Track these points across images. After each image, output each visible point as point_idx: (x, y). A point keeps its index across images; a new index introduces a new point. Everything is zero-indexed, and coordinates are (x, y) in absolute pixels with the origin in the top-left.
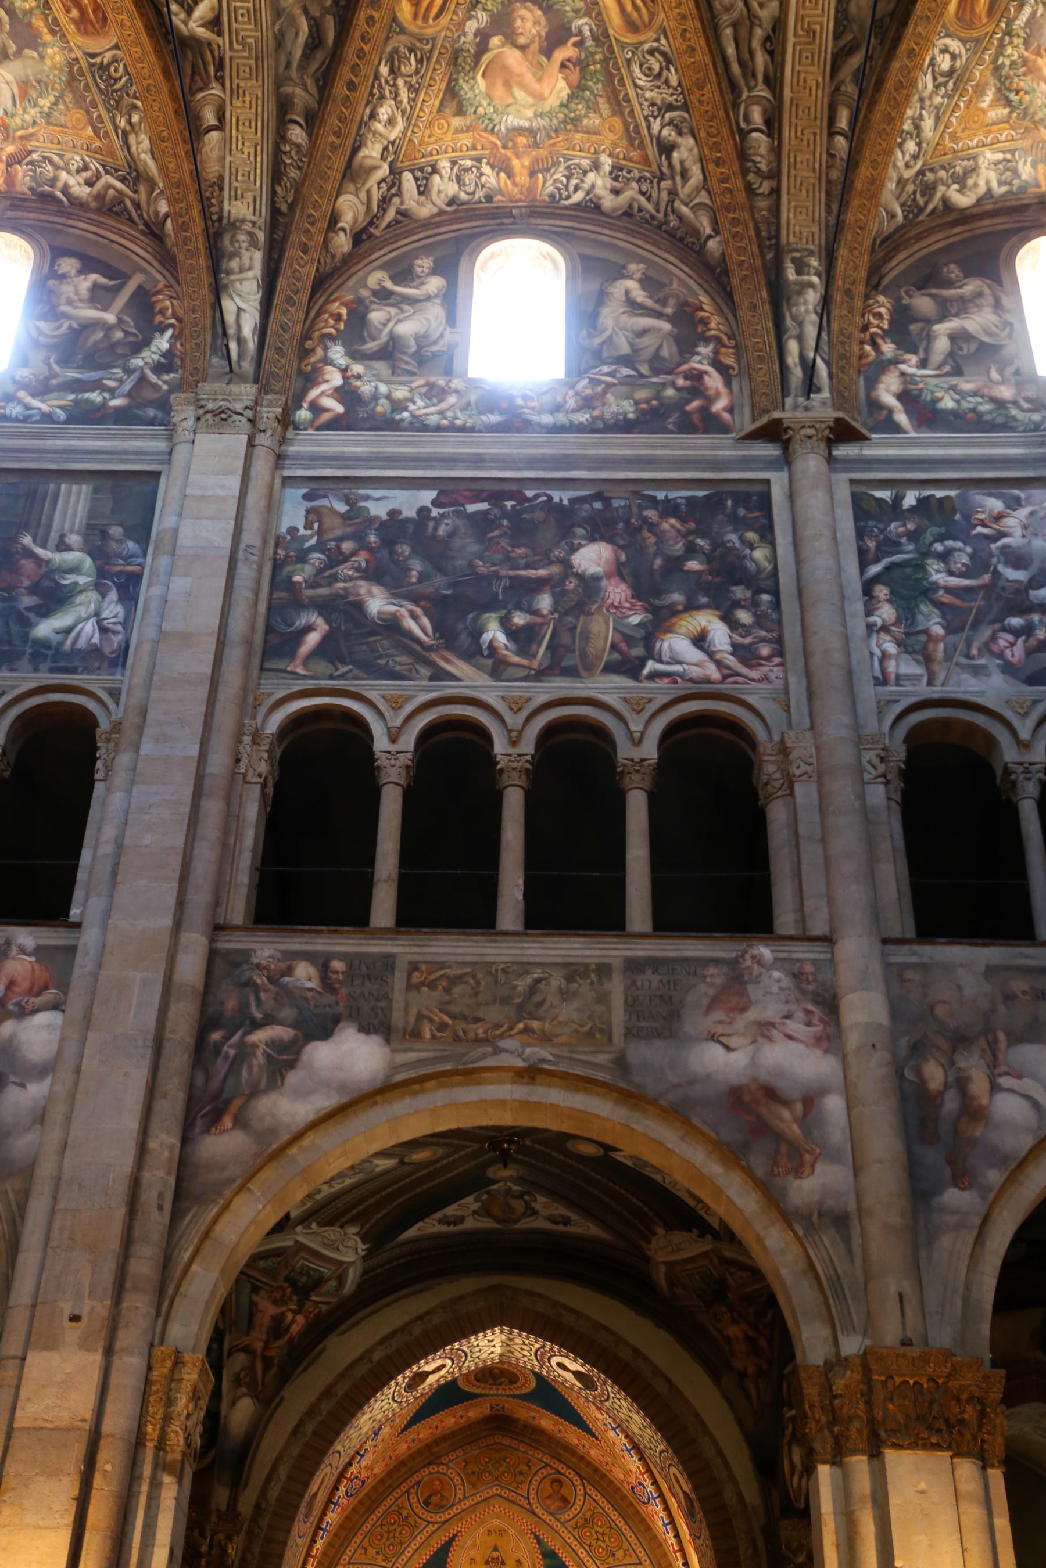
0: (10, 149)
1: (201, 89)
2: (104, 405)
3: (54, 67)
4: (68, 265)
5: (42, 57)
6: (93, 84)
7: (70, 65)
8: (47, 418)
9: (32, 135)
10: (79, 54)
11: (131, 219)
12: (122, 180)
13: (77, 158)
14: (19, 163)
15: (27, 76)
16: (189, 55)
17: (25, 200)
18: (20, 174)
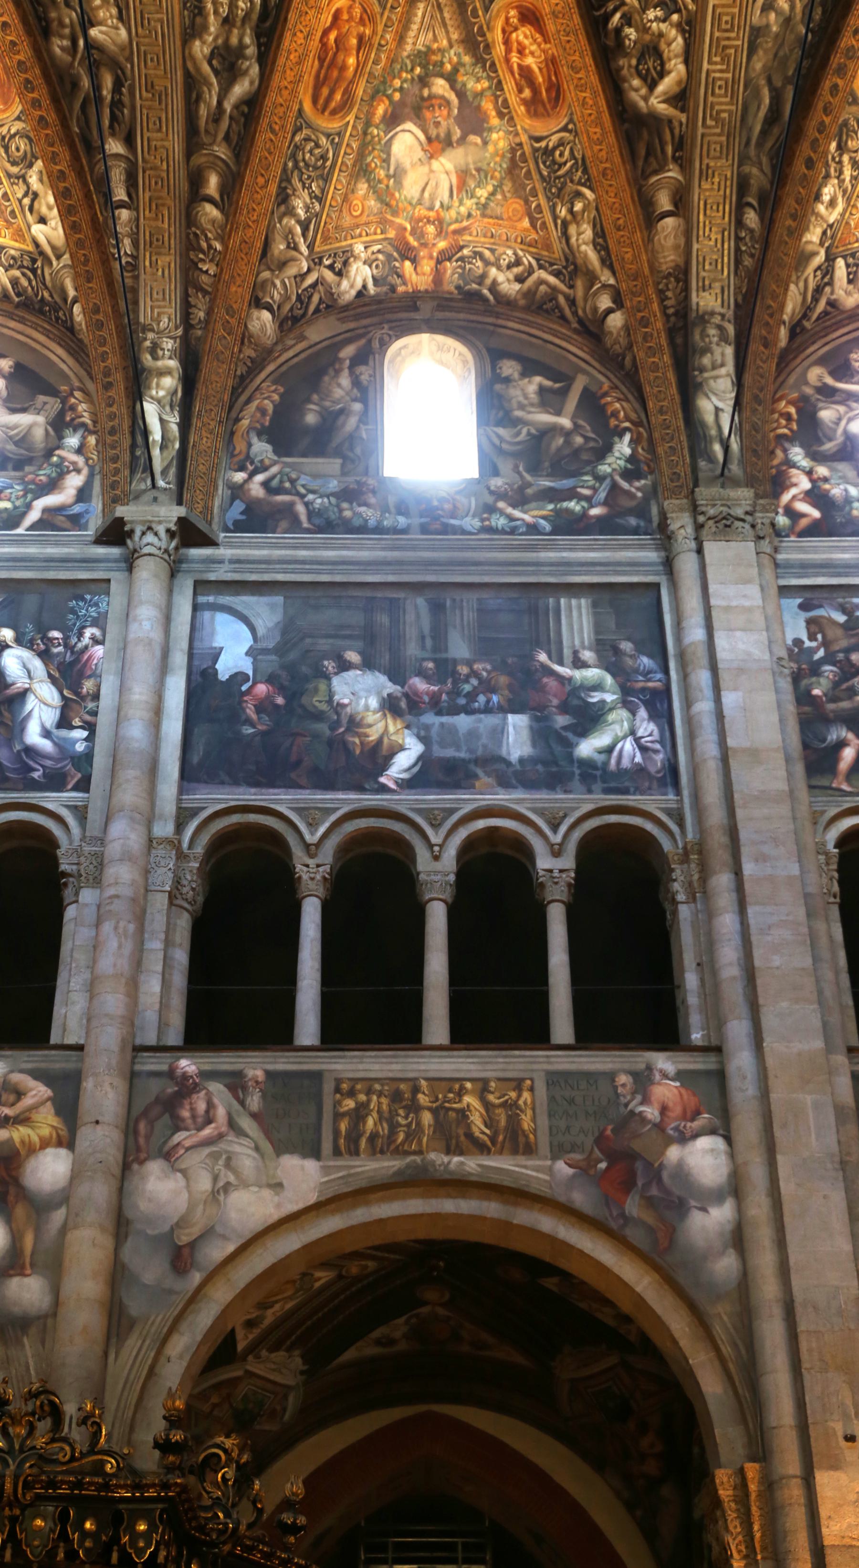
0: (442, 245)
2: (584, 514)
3: (496, 153)
4: (509, 368)
5: (485, 143)
6: (538, 172)
7: (513, 151)
8: (533, 529)
9: (465, 229)
10: (524, 138)
12: (557, 274)
13: (510, 252)
14: (449, 259)
15: (467, 164)
17: (451, 300)
18: (449, 272)
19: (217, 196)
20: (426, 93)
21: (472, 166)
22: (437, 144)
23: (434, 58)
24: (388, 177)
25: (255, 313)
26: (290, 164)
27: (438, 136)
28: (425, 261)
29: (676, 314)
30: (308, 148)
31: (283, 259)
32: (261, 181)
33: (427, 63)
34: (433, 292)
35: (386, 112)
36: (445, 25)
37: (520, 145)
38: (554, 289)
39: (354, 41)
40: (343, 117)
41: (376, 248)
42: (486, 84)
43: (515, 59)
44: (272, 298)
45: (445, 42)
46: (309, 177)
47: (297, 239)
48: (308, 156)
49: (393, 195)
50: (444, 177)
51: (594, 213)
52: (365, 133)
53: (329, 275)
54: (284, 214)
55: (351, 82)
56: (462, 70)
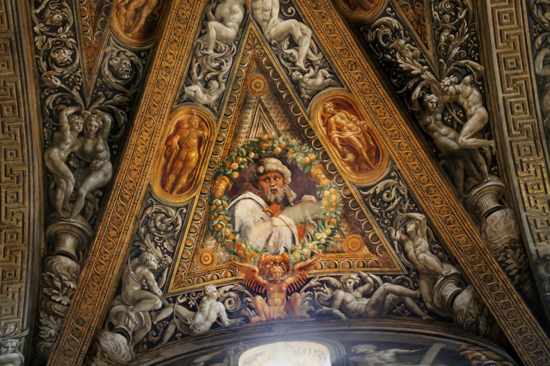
0: (290, 280)
1: (476, 186)
3: (330, 205)
5: (319, 199)
9: (310, 265)
10: (353, 190)
11: (414, 315)
12: (401, 283)
13: (354, 276)
14: (298, 291)
15: (305, 217)
16: (461, 164)
19: (73, 252)
20: (261, 169)
21: (310, 218)
22: (276, 206)
23: (265, 145)
24: (234, 233)
25: (109, 335)
26: (143, 230)
27: (276, 200)
28: (276, 295)
29: (520, 272)
30: (159, 218)
31: (137, 297)
32: (113, 233)
33: (260, 151)
34: (286, 318)
35: (227, 187)
36: (272, 122)
37: (351, 195)
38: (400, 295)
39: (195, 141)
40: (190, 194)
41: (227, 288)
42: (313, 156)
43: (335, 135)
44: (127, 326)
45: (274, 133)
46: (161, 238)
47: (151, 283)
48: (159, 224)
49: (240, 246)
50: (285, 229)
51: (426, 228)
52: (210, 204)
53: (184, 311)
54: (138, 265)
55: (195, 169)
56: (291, 150)
